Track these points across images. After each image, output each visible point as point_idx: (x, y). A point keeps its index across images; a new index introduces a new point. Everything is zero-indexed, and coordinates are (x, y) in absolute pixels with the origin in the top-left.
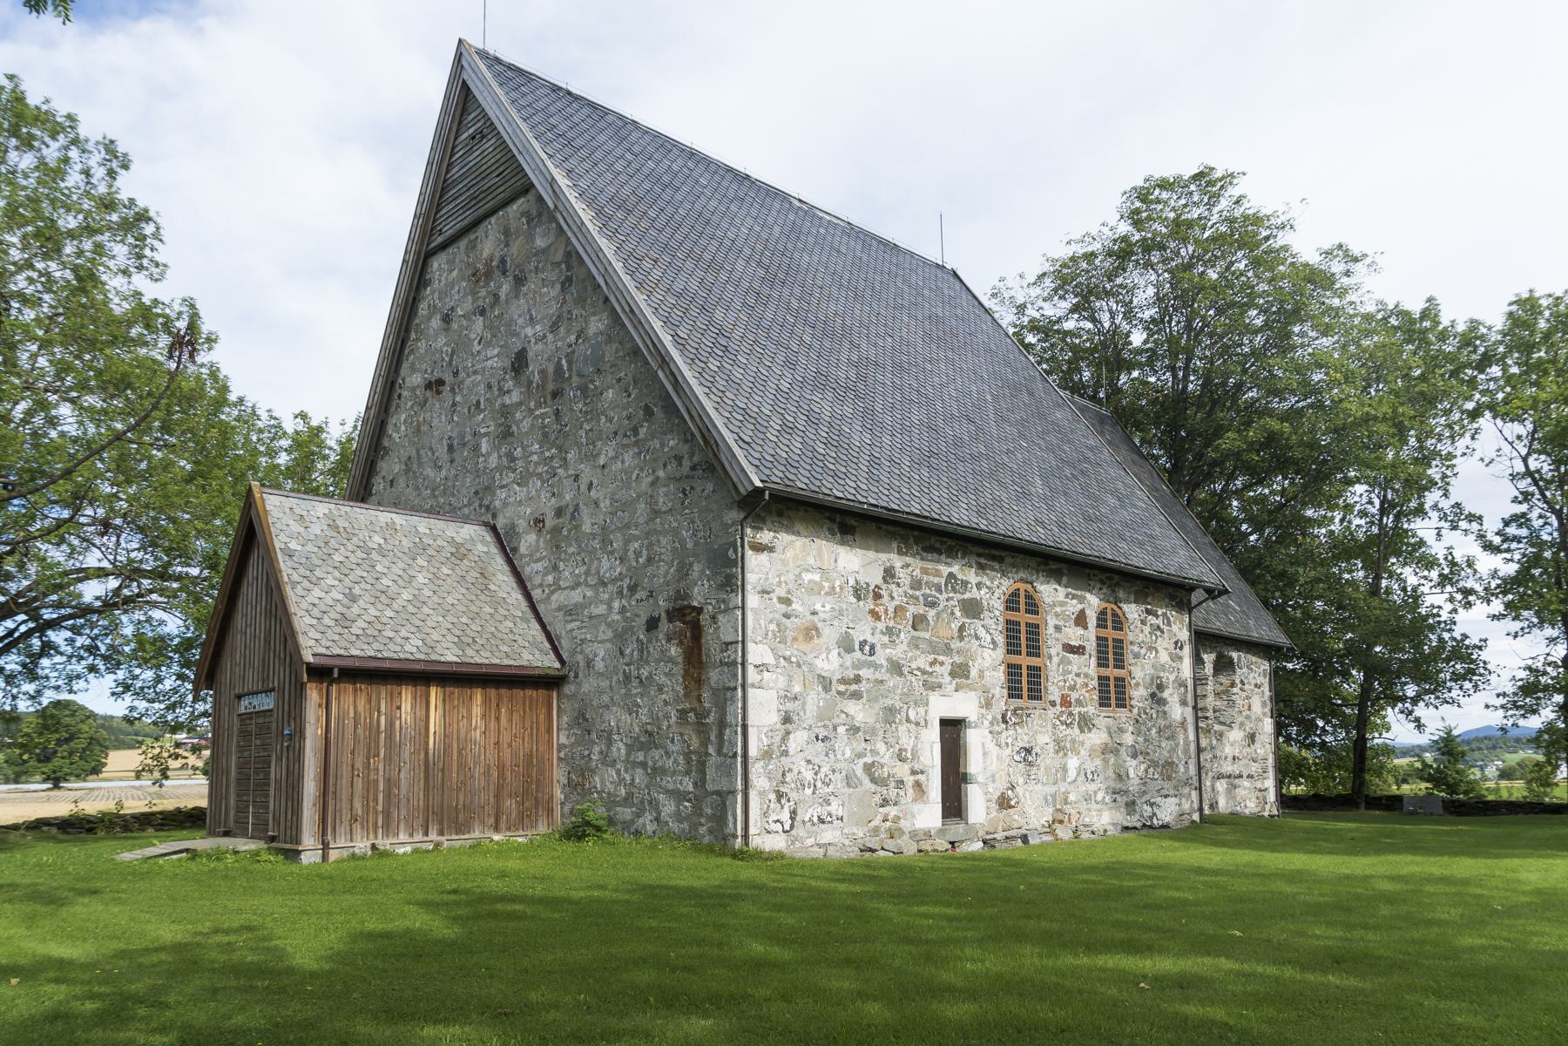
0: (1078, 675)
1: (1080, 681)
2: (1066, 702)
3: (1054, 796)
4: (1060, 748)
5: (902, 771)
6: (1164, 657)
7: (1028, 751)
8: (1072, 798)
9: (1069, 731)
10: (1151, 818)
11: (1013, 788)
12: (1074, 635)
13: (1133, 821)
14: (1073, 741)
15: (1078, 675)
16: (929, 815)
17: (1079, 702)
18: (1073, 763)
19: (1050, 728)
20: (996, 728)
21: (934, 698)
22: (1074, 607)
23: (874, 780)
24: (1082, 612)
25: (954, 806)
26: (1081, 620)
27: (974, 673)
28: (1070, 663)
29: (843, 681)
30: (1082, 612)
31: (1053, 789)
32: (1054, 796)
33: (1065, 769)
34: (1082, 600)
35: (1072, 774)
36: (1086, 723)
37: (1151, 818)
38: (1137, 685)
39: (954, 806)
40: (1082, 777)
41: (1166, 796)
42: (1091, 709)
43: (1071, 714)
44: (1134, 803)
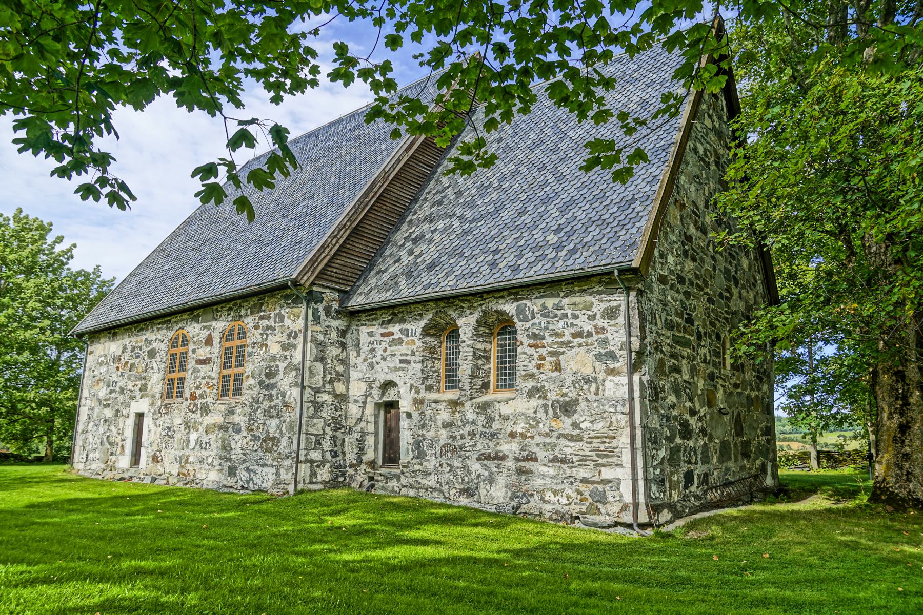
0: (203, 378)
1: (203, 382)
2: (193, 397)
3: (180, 457)
4: (187, 424)
5: (118, 439)
6: (275, 349)
7: (169, 429)
8: (191, 459)
9: (193, 416)
10: (248, 482)
11: (160, 451)
12: (203, 352)
13: (231, 481)
14: (195, 422)
15: (203, 378)
16: (124, 462)
17: (201, 396)
18: (193, 436)
19: (183, 414)
20: (156, 417)
21: (133, 404)
22: (205, 334)
23: (110, 444)
24: (210, 336)
25: (136, 459)
26: (209, 342)
27: (149, 387)
28: (199, 371)
29: (105, 400)
30: (210, 336)
31: (179, 453)
32: (180, 457)
33: (188, 441)
34: (208, 328)
35: (192, 444)
36: (206, 410)
37: (248, 482)
38: (248, 377)
39: (136, 459)
40: (197, 447)
41: (263, 465)
42: (210, 400)
43: (195, 405)
44: (235, 468)
